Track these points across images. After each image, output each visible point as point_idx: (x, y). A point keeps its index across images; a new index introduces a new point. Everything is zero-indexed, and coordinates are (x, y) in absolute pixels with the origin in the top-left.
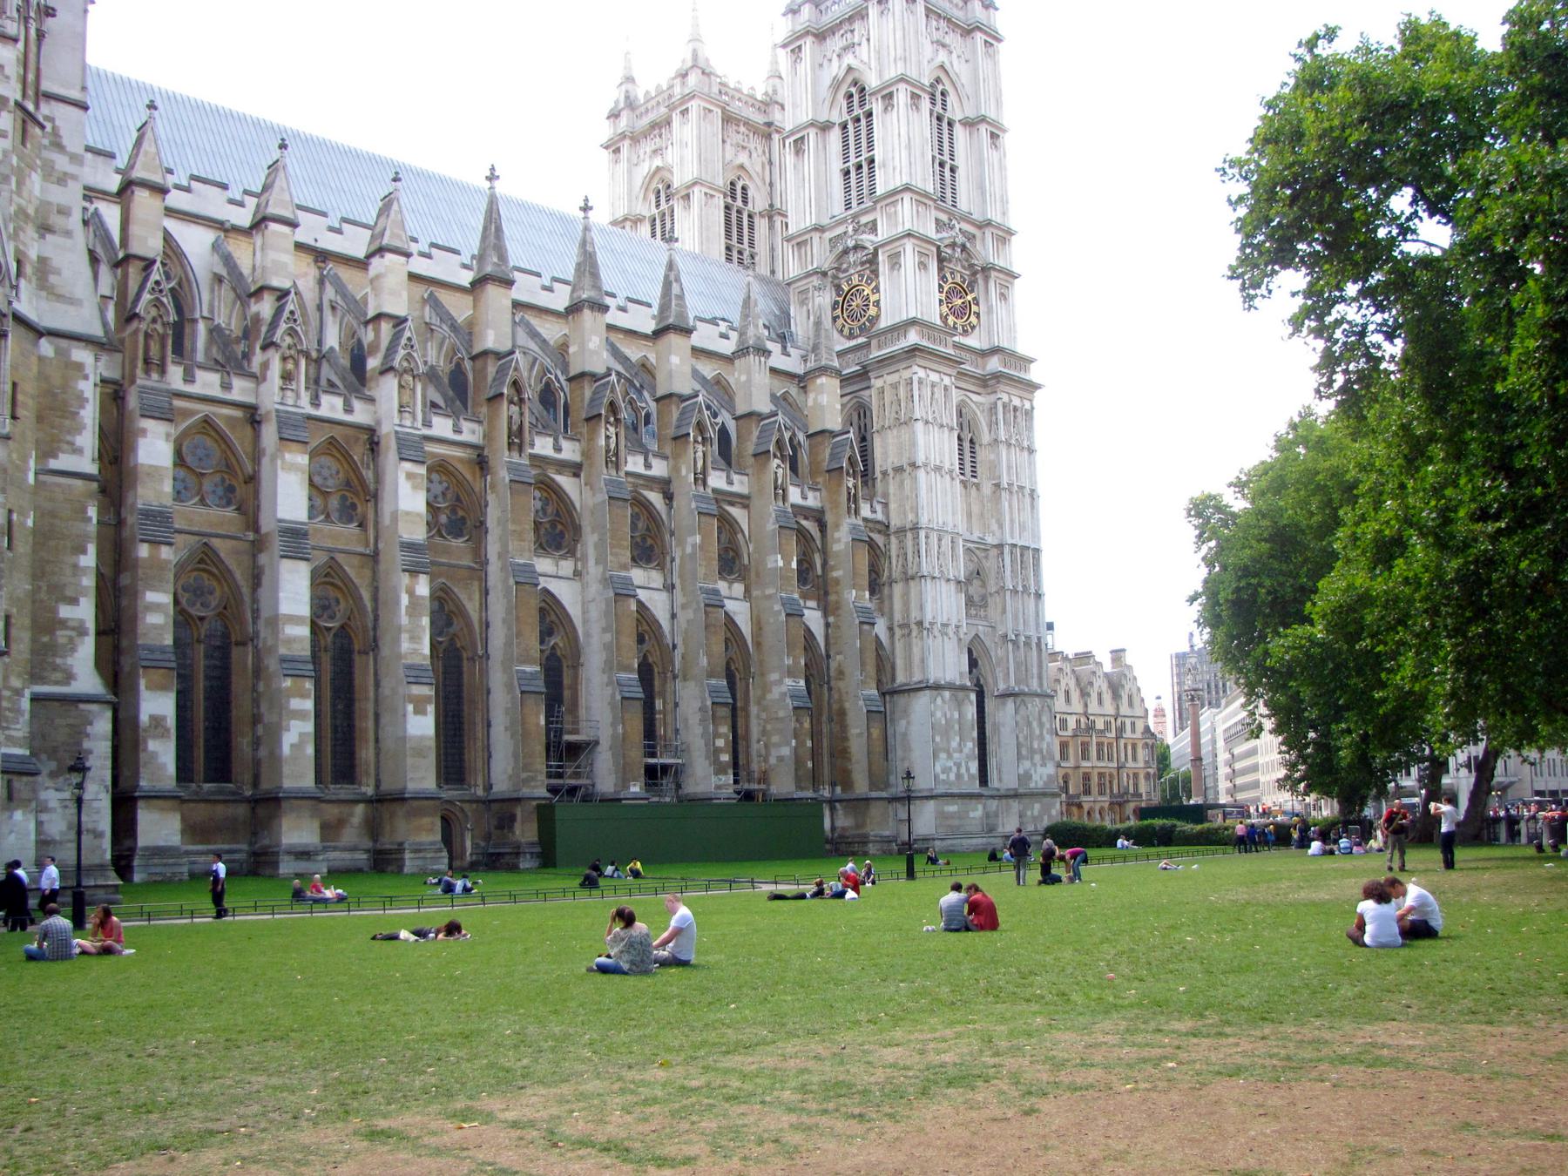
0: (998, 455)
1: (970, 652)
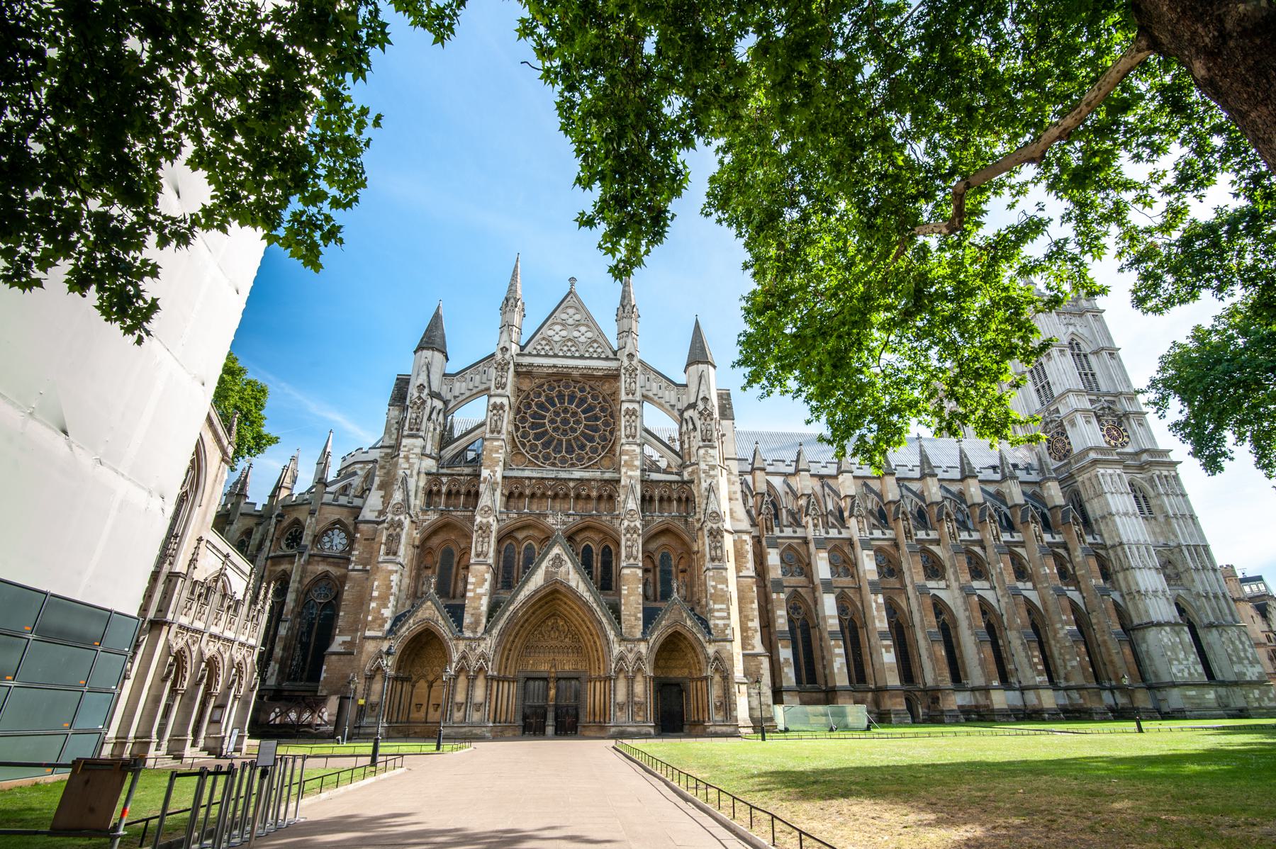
0: (1163, 502)
1: (1177, 605)
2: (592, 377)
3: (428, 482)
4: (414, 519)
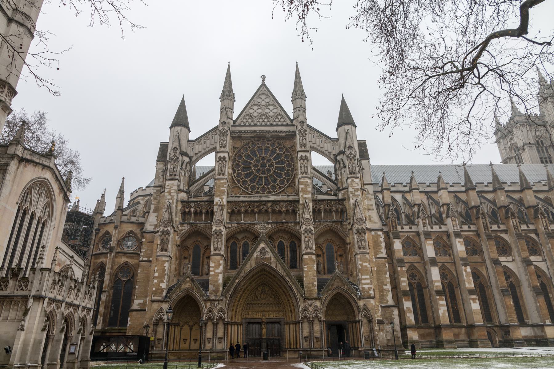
2: (279, 137)
3: (183, 207)
4: (176, 229)
